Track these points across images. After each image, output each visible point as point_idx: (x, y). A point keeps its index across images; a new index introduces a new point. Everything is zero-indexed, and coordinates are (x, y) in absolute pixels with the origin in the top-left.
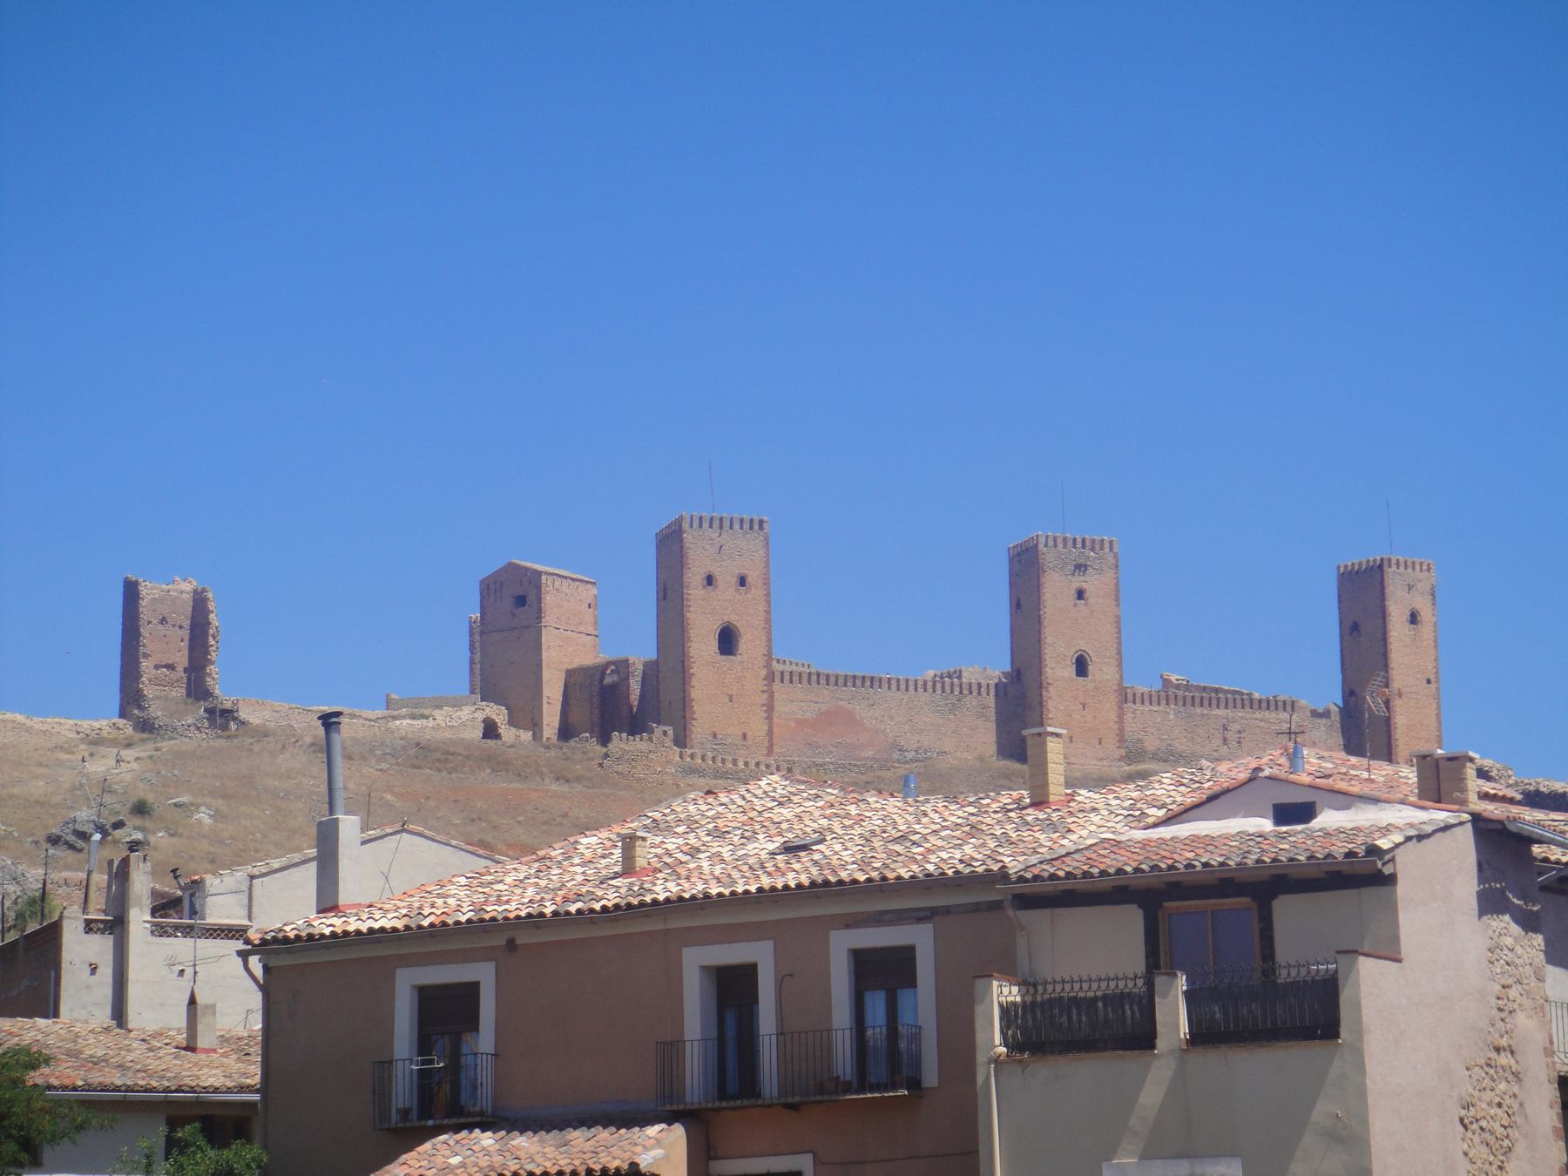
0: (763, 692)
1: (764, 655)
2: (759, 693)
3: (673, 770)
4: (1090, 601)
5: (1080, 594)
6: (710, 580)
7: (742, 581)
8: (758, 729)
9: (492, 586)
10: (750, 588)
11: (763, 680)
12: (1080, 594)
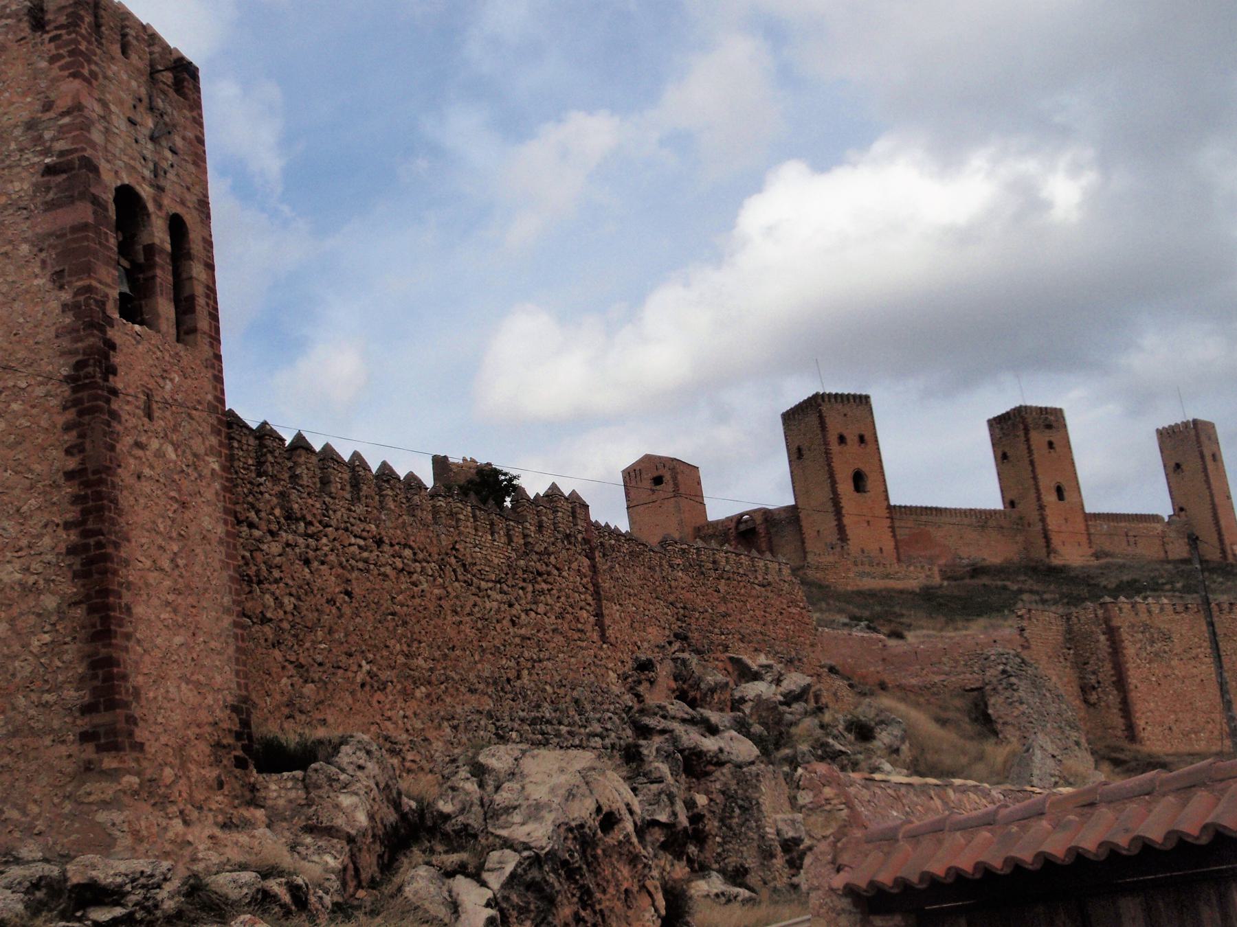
5: (1051, 445)
6: (842, 439)
7: (862, 439)
8: (889, 545)
9: (632, 474)
10: (867, 444)
12: (1051, 445)
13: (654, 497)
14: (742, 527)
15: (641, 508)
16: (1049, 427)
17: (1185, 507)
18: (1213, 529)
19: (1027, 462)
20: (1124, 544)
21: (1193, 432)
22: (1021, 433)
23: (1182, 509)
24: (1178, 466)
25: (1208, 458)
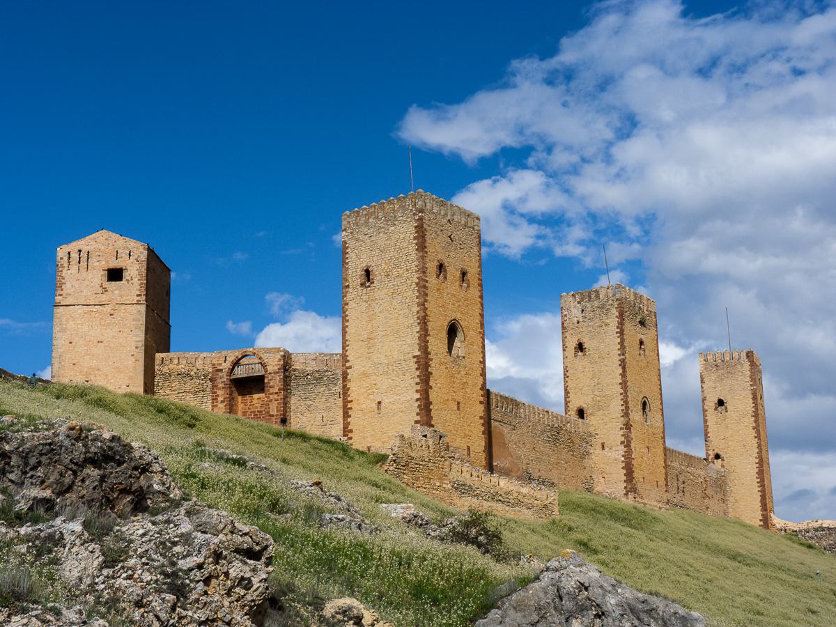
0: (481, 402)
1: (480, 362)
2: (478, 403)
3: (449, 486)
4: (647, 351)
5: (641, 343)
6: (441, 267)
7: (464, 274)
10: (468, 286)
11: (480, 389)
12: (641, 343)
13: (104, 298)
14: (240, 372)
15: (80, 310)
16: (642, 323)
17: (722, 455)
18: (756, 489)
19: (616, 359)
20: (675, 490)
21: (747, 365)
22: (613, 321)
23: (717, 456)
24: (721, 403)
25: (759, 401)
